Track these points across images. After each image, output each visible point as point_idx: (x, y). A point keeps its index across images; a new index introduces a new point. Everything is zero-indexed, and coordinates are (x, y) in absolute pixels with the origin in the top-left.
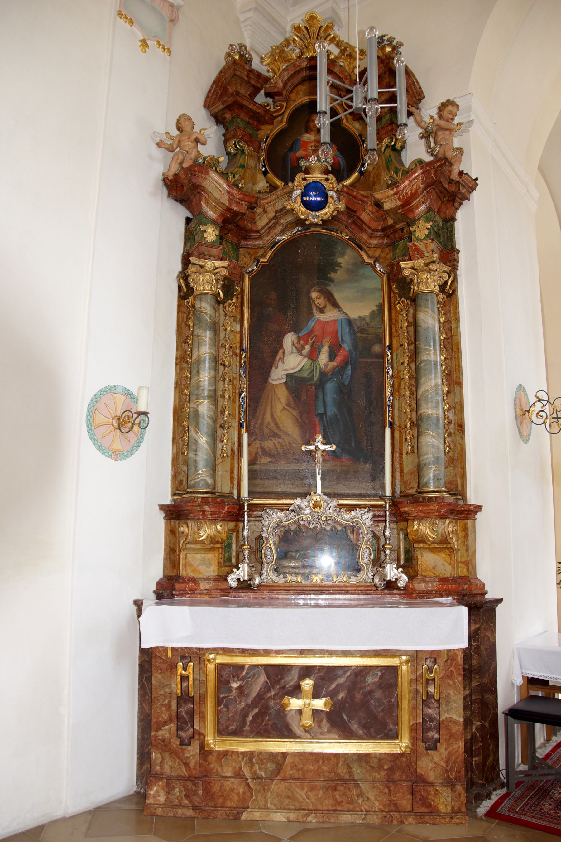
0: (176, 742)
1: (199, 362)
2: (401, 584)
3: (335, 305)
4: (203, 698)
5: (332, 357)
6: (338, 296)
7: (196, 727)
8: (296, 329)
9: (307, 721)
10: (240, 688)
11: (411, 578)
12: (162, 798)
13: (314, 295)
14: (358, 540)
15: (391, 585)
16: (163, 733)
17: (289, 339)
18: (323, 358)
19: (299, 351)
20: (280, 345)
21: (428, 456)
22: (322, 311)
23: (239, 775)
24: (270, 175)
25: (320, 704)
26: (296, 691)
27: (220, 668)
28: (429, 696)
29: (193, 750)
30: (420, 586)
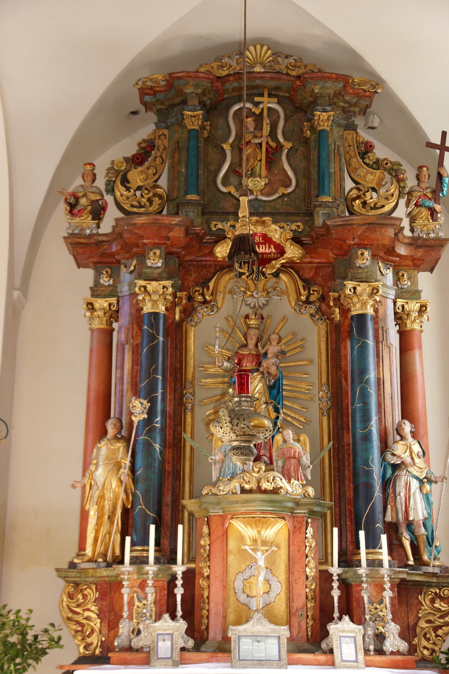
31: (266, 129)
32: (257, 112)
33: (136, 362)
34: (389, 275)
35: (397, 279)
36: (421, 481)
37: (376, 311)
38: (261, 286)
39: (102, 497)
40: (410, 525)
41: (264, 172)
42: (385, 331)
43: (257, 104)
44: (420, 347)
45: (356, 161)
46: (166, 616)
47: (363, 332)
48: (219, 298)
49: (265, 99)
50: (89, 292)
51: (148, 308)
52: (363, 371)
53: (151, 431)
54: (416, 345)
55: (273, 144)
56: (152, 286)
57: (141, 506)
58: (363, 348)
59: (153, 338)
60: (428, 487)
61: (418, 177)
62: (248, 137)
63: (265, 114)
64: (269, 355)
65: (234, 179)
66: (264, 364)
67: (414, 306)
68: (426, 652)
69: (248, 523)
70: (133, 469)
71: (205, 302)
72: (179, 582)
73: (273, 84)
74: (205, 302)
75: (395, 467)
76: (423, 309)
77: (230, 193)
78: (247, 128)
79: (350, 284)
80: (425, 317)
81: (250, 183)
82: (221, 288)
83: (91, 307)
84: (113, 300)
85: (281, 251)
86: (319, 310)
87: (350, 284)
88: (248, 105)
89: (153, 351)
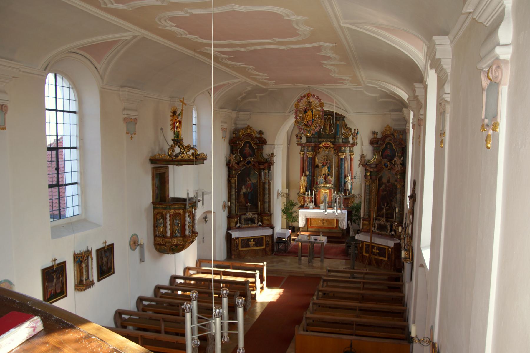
0: (236, 250)
1: (233, 195)
2: (261, 225)
3: (251, 180)
4: (239, 244)
5: (250, 189)
6: (251, 179)
7: (238, 247)
8: (245, 185)
9: (252, 245)
10: (244, 242)
11: (263, 224)
12: (234, 257)
13: (247, 179)
14: (255, 219)
15: (260, 225)
16: (234, 249)
17: (243, 187)
18: (249, 190)
19: (245, 188)
20: (242, 188)
21: (265, 207)
22: (248, 181)
23: (244, 253)
24: (240, 156)
25: (254, 243)
26: (251, 241)
27: (241, 239)
28: (267, 241)
29: (238, 250)
30: (264, 225)
31: (329, 121)
32: (328, 118)
33: (307, 164)
34: (348, 148)
35: (350, 149)
36: (350, 184)
37: (345, 157)
38: (327, 150)
39: (303, 185)
40: (348, 190)
41: (329, 129)
42: (347, 159)
43: (327, 117)
44: (353, 160)
45: (344, 127)
46: (311, 203)
47: (342, 161)
48: (321, 152)
49: (329, 116)
50: (300, 151)
51: (309, 156)
52: (342, 167)
53: (309, 176)
54: (352, 160)
55: (330, 124)
56: (309, 153)
57: (308, 187)
58: (342, 163)
59: (309, 161)
60: (351, 184)
61: (354, 131)
62: (326, 123)
63: (329, 119)
64: (328, 163)
65: (324, 131)
66: (327, 165)
67: (352, 154)
68: (349, 206)
69: (323, 190)
70: (307, 181)
71: (318, 153)
72: (313, 198)
73: (330, 114)
74: (318, 153)
75: (346, 181)
76: (353, 154)
77: (323, 133)
78: (326, 121)
79: (340, 153)
80: (354, 155)
81: (326, 131)
82: (321, 150)
83: (300, 153)
84: (304, 152)
85: (330, 146)
86: (337, 154)
87: (340, 153)
88: (326, 117)
89: (309, 164)
